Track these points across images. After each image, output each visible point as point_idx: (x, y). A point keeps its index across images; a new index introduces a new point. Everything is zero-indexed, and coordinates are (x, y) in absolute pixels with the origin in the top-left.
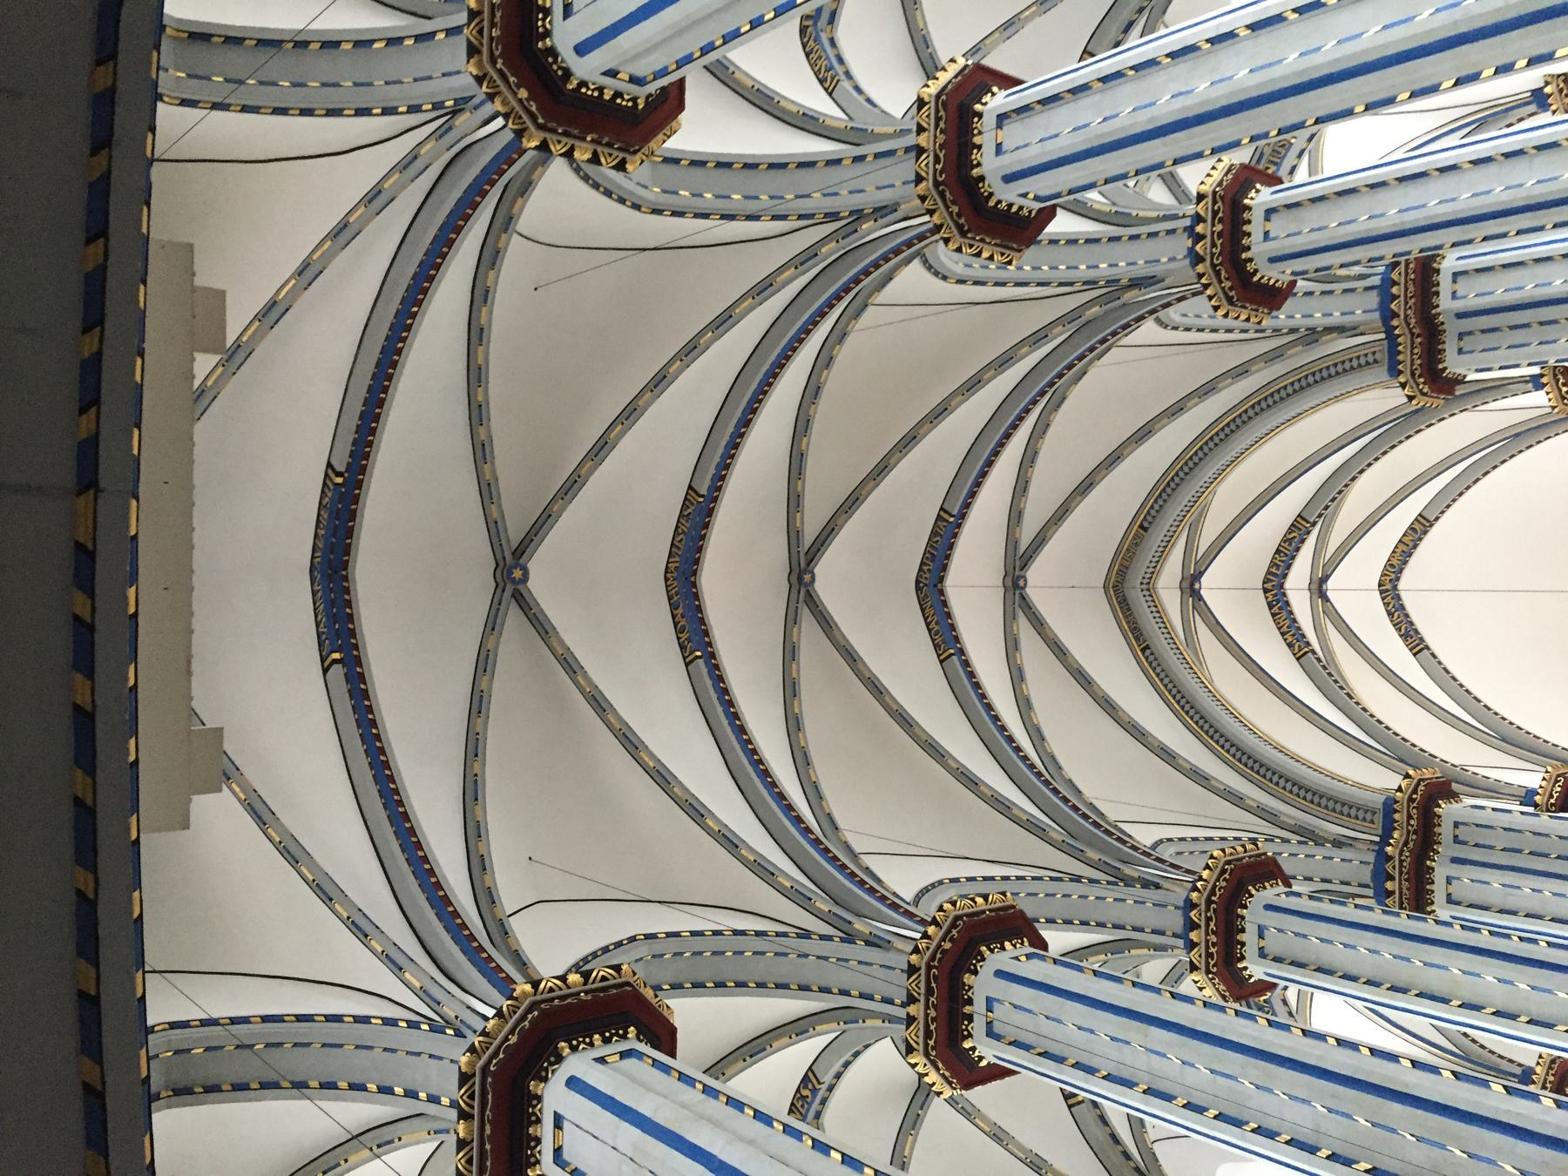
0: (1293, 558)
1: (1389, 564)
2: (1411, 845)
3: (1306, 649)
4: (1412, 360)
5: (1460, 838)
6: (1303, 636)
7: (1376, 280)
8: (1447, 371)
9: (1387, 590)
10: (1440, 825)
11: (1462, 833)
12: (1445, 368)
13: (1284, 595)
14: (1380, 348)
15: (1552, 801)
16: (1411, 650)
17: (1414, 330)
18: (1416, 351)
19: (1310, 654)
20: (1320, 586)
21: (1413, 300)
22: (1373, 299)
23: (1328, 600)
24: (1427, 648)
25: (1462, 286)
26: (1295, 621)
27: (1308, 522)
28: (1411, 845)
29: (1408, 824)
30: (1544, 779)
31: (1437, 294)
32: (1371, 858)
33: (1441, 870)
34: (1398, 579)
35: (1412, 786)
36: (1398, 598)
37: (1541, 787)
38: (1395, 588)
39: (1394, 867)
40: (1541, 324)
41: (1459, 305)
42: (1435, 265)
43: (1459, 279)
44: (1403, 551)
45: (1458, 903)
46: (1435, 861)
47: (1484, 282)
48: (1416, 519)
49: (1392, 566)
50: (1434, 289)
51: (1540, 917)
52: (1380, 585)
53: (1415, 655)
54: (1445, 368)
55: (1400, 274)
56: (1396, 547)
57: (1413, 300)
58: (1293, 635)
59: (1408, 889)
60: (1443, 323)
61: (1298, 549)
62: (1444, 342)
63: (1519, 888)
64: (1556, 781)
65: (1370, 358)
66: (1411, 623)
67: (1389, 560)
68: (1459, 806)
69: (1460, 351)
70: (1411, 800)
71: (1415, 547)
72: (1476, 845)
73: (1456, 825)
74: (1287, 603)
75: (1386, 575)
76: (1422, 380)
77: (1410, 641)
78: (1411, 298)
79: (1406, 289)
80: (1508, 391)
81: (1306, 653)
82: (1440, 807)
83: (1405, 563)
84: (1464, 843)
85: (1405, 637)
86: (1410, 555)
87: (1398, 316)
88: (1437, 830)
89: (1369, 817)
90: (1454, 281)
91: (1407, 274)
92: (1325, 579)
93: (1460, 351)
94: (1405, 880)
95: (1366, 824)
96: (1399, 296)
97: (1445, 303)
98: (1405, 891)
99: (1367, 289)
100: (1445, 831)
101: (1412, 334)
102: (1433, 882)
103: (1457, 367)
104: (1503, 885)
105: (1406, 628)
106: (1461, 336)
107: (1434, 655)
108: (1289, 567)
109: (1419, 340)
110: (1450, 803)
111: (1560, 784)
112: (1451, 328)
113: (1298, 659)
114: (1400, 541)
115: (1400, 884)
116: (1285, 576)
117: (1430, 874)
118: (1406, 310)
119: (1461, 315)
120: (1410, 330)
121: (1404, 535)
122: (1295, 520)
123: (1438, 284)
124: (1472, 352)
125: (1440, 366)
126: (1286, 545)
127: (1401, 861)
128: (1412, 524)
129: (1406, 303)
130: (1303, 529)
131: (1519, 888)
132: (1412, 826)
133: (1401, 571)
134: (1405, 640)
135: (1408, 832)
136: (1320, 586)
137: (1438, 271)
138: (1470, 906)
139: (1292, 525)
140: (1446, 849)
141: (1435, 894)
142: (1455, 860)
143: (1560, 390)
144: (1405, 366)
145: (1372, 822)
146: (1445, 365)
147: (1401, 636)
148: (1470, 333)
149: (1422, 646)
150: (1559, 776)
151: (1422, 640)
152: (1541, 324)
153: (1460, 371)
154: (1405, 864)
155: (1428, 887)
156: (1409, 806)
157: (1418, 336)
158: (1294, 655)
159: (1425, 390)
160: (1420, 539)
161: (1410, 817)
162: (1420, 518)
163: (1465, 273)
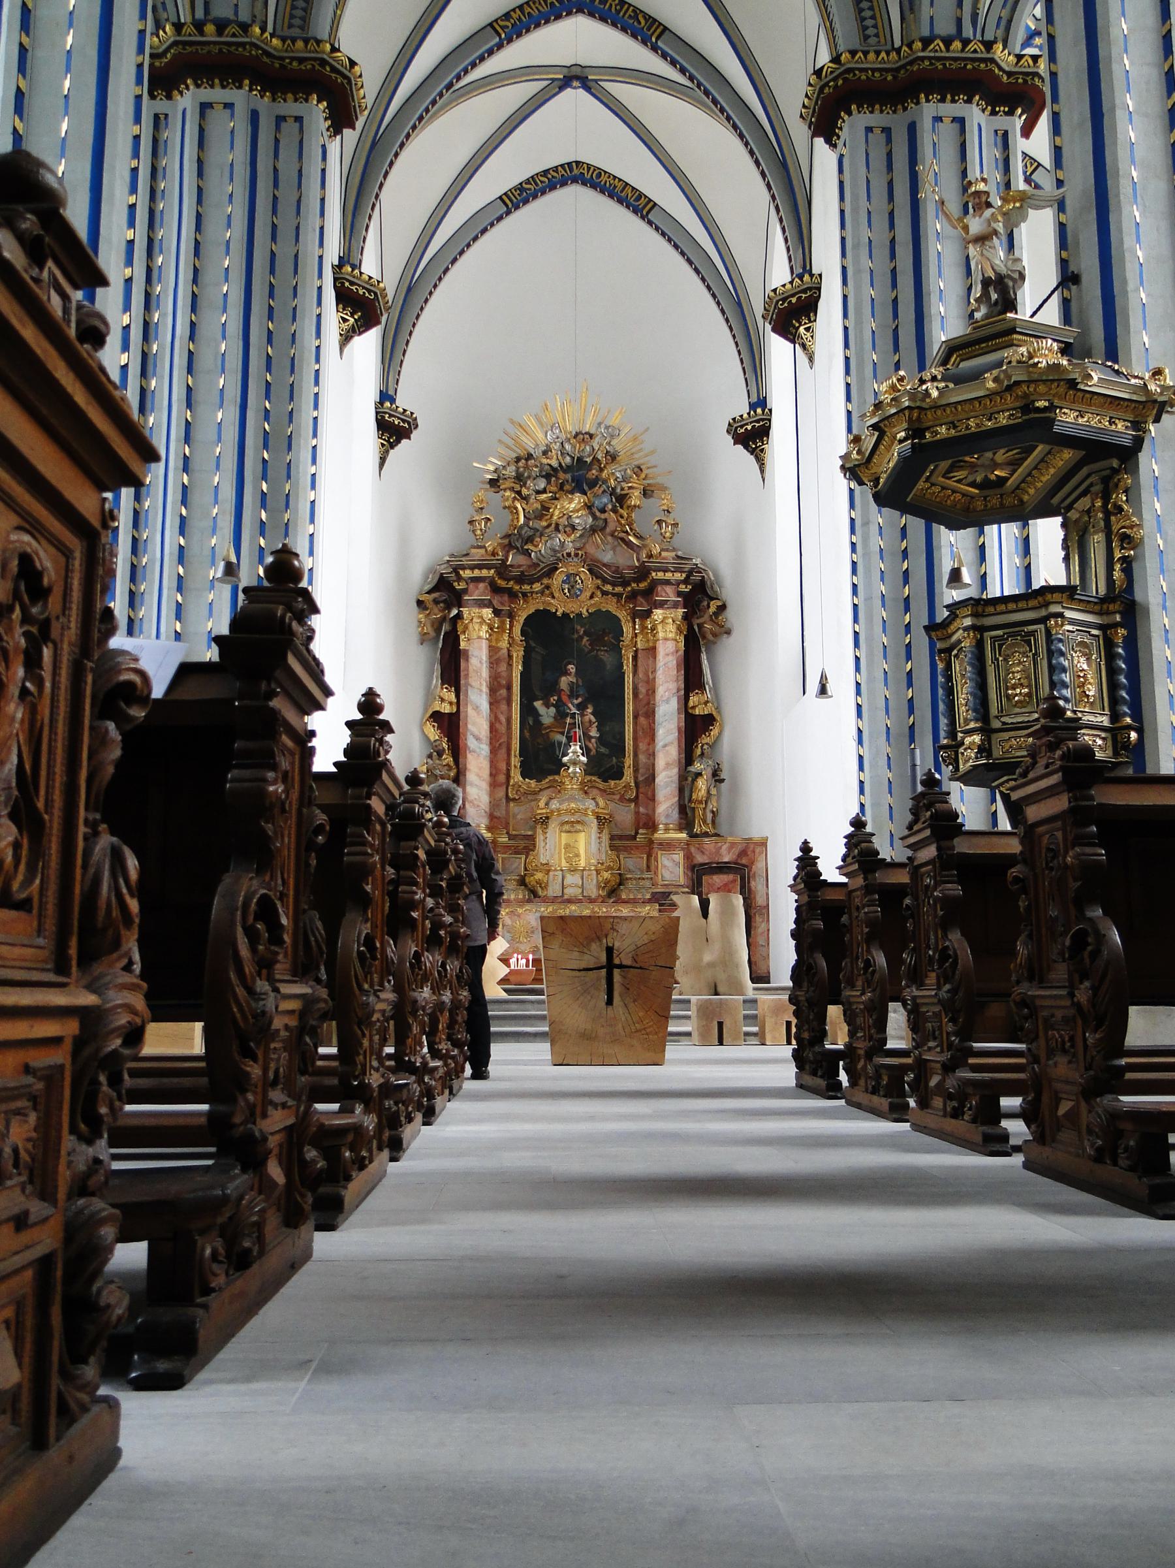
0: (614, 25)
1: (600, 172)
2: (265, 59)
3: (503, 36)
4: (865, 70)
5: (283, 125)
6: (519, 35)
7: (968, 31)
8: (846, 117)
9: (571, 170)
10: (296, 100)
11: (290, 127)
12: (850, 114)
13: (569, 14)
14: (883, 40)
15: (347, 284)
16: (505, 194)
17: (902, 72)
18: (877, 75)
19: (497, 39)
20: (577, 78)
21: (940, 67)
22: (945, 27)
23: (561, 89)
24: (508, 213)
25: (948, 128)
26: (538, 25)
27: (657, 39)
28: (265, 59)
29: (293, 59)
30: (370, 278)
31: (943, 100)
32: (244, 16)
33: (241, 97)
34: (584, 184)
35: (339, 67)
36: (564, 183)
37: (361, 273)
38: (575, 180)
39: (234, 35)
40: (891, 214)
41: (926, 123)
42: (977, 97)
43: (956, 126)
44: (615, 187)
45: (202, 115)
46: (251, 90)
47: (949, 151)
48: (650, 200)
49: (599, 175)
50: (949, 97)
51: (200, 201)
52: (577, 163)
53: (500, 198)
54: (850, 114)
55: (975, 51)
56: (620, 180)
57: (940, 67)
58: (520, 19)
59: (209, 52)
60: (905, 109)
61: (624, 30)
62: (882, 111)
63: (232, 180)
64: (369, 291)
65: (871, 31)
66: (535, 197)
67: (605, 172)
68: (326, 134)
69: (869, 130)
70: (323, 63)
71: (620, 201)
72: (277, 141)
73: (299, 119)
74: (558, 17)
75: (589, 169)
76: (840, 82)
77: (516, 194)
78: (944, 65)
79: (955, 59)
80: (795, 251)
81: (499, 35)
82: (319, 101)
83: (602, 192)
84: (278, 128)
85: (520, 188)
86: (611, 196)
87: (923, 50)
88: (290, 96)
89: (297, 22)
90: (954, 120)
91: (973, 60)
92: (586, 84)
93: (869, 130)
94: (220, 50)
95: (286, 20)
96: (948, 50)
97: (928, 109)
98: (206, 49)
99: (959, 22)
100: (290, 107)
101: (898, 70)
102: (223, 87)
103: (851, 127)
104: (232, 165)
105: (530, 189)
106: (887, 131)
107: (500, 219)
108: (603, 19)
109: (890, 78)
110: (326, 119)
111: (367, 295)
112: (896, 120)
113: (491, 25)
114: (627, 184)
115: (215, 43)
116: (591, 15)
117: (233, 83)
118: (929, 58)
119: (912, 129)
120: (904, 66)
121: (633, 188)
122: (660, 24)
123: (953, 101)
124: (867, 141)
125: (854, 107)
126: (630, 12)
127: (243, 45)
128: (646, 197)
129: (939, 59)
130: (650, 33)
131: (232, 180)
132: (290, 63)
133: (594, 186)
134: (515, 188)
135: (283, 59)
136: (577, 78)
137: (969, 101)
138: (202, 130)
139: (655, 20)
140: (264, 104)
141: (209, 90)
142: (254, 117)
143: (793, 295)
144: (860, 61)
145: (290, 26)
146: (855, 112)
147: (521, 184)
148: (889, 140)
149: (510, 206)
150: (376, 294)
151: (517, 207)
152: (891, 214)
153: (844, 134)
154: (240, 49)
155: (217, 81)
156: (315, 59)
157: (895, 77)
158: (496, 21)
159: (826, 90)
160: (628, 207)
161: (301, 60)
162: (652, 203)
163: (963, 131)
